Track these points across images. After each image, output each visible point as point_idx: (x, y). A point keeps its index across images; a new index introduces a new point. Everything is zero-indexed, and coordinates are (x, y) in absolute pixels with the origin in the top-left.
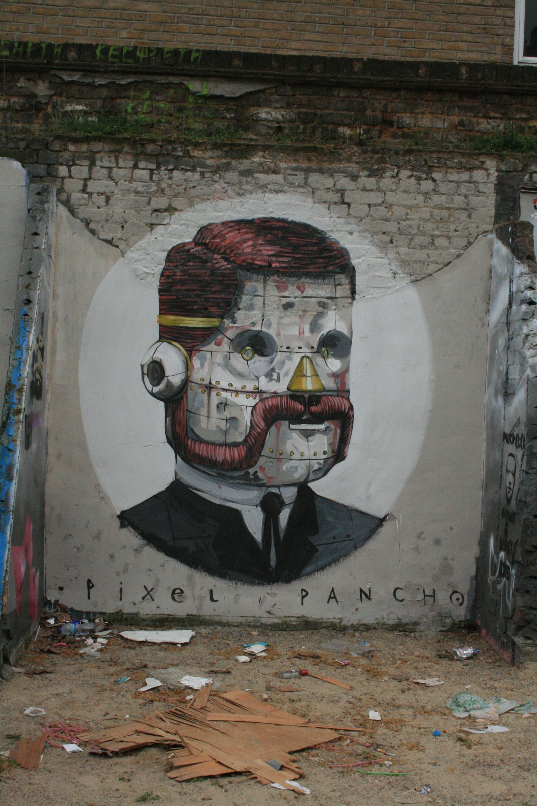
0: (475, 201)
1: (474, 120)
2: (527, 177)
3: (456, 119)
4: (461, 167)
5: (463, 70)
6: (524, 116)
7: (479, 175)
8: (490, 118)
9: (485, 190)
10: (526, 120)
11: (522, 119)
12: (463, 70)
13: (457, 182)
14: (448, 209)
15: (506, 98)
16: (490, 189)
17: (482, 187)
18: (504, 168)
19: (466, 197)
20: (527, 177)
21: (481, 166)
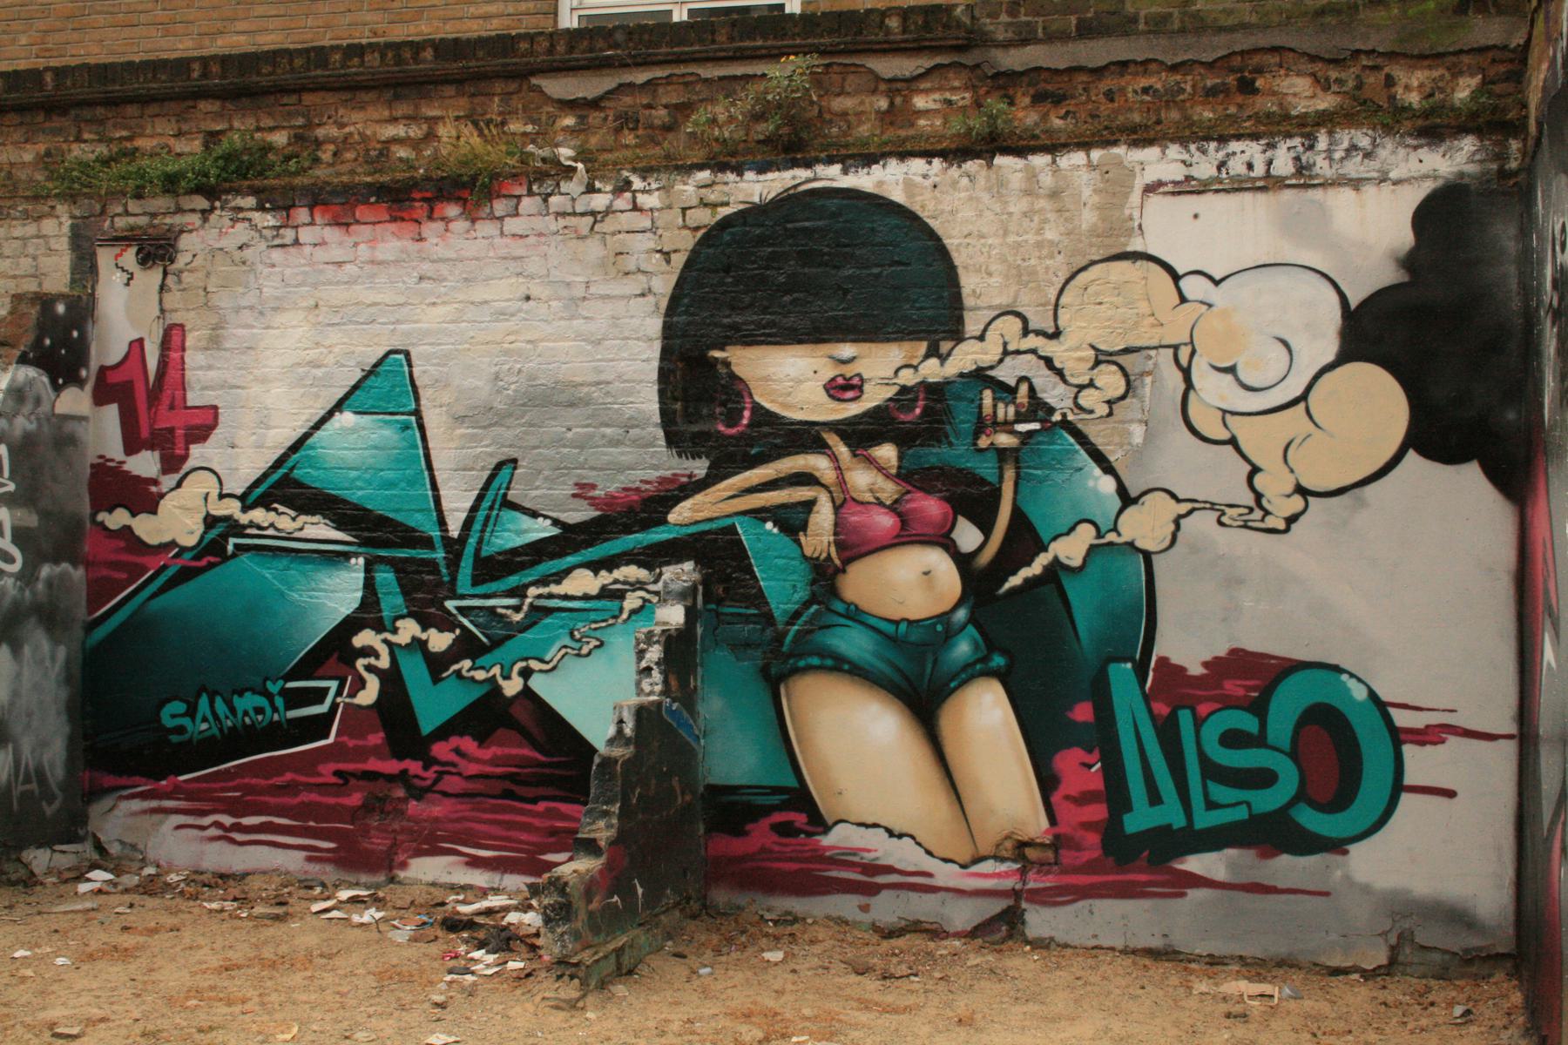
0: (46, 262)
1: (65, 146)
2: (107, 223)
3: (42, 148)
4: (26, 216)
5: (48, 78)
6: (125, 133)
7: (48, 226)
8: (85, 141)
9: (57, 247)
10: (130, 139)
11: (122, 139)
12: (48, 78)
13: (23, 239)
14: (14, 277)
15: (100, 111)
16: (63, 244)
17: (54, 244)
18: (77, 213)
19: (35, 258)
20: (107, 223)
21: (52, 213)
